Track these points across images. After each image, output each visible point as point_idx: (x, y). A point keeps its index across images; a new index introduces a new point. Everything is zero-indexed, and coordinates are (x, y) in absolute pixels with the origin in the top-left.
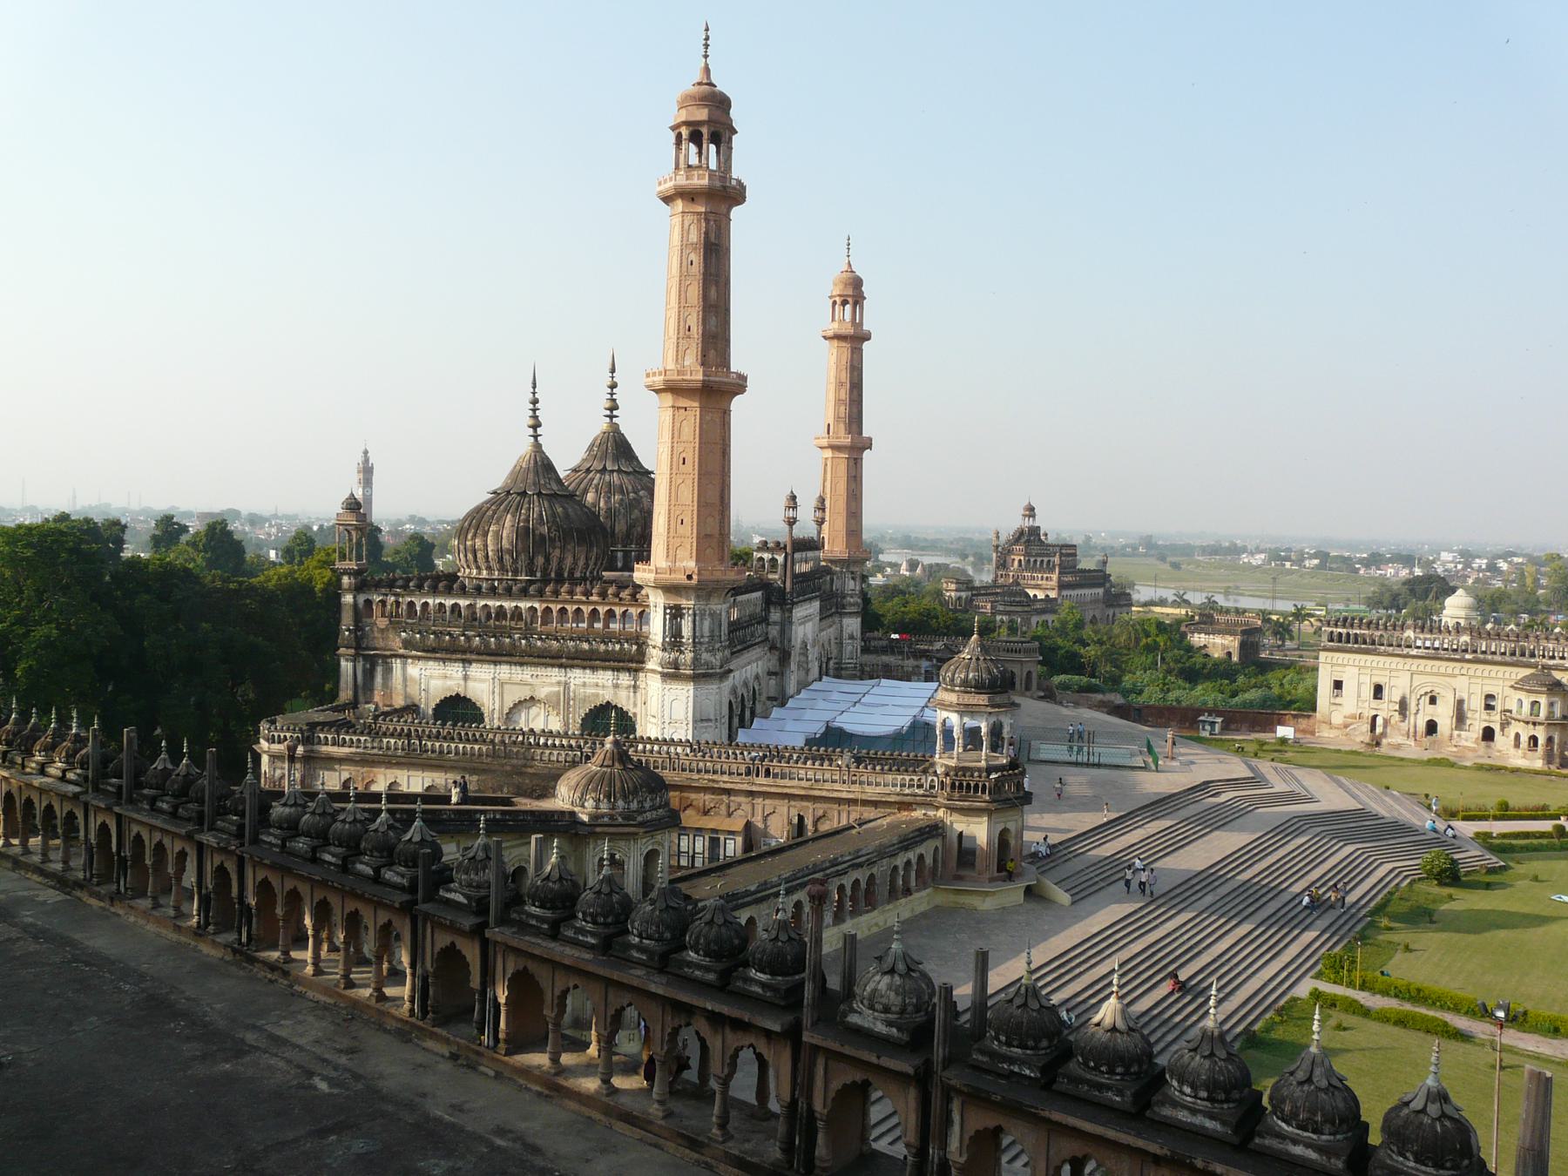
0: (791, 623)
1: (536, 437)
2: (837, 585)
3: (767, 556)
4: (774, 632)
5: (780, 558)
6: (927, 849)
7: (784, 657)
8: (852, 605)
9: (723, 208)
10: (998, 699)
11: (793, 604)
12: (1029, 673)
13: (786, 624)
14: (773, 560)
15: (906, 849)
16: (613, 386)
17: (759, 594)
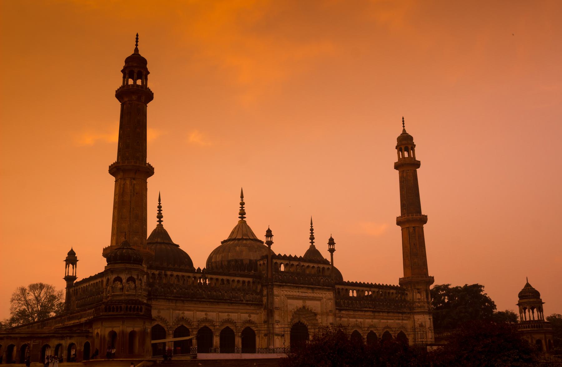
0: (272, 295)
1: (160, 221)
2: (409, 297)
3: (262, 262)
4: (265, 300)
5: (266, 262)
6: (79, 342)
7: (270, 313)
8: (420, 307)
9: (134, 97)
10: (117, 266)
11: (273, 285)
12: (539, 342)
13: (271, 295)
14: (264, 263)
15: (57, 337)
16: (242, 204)
17: (247, 279)
